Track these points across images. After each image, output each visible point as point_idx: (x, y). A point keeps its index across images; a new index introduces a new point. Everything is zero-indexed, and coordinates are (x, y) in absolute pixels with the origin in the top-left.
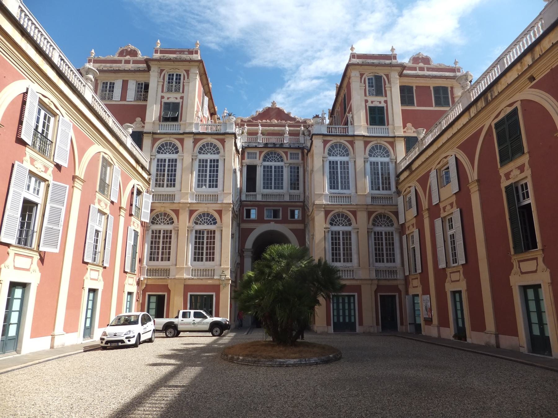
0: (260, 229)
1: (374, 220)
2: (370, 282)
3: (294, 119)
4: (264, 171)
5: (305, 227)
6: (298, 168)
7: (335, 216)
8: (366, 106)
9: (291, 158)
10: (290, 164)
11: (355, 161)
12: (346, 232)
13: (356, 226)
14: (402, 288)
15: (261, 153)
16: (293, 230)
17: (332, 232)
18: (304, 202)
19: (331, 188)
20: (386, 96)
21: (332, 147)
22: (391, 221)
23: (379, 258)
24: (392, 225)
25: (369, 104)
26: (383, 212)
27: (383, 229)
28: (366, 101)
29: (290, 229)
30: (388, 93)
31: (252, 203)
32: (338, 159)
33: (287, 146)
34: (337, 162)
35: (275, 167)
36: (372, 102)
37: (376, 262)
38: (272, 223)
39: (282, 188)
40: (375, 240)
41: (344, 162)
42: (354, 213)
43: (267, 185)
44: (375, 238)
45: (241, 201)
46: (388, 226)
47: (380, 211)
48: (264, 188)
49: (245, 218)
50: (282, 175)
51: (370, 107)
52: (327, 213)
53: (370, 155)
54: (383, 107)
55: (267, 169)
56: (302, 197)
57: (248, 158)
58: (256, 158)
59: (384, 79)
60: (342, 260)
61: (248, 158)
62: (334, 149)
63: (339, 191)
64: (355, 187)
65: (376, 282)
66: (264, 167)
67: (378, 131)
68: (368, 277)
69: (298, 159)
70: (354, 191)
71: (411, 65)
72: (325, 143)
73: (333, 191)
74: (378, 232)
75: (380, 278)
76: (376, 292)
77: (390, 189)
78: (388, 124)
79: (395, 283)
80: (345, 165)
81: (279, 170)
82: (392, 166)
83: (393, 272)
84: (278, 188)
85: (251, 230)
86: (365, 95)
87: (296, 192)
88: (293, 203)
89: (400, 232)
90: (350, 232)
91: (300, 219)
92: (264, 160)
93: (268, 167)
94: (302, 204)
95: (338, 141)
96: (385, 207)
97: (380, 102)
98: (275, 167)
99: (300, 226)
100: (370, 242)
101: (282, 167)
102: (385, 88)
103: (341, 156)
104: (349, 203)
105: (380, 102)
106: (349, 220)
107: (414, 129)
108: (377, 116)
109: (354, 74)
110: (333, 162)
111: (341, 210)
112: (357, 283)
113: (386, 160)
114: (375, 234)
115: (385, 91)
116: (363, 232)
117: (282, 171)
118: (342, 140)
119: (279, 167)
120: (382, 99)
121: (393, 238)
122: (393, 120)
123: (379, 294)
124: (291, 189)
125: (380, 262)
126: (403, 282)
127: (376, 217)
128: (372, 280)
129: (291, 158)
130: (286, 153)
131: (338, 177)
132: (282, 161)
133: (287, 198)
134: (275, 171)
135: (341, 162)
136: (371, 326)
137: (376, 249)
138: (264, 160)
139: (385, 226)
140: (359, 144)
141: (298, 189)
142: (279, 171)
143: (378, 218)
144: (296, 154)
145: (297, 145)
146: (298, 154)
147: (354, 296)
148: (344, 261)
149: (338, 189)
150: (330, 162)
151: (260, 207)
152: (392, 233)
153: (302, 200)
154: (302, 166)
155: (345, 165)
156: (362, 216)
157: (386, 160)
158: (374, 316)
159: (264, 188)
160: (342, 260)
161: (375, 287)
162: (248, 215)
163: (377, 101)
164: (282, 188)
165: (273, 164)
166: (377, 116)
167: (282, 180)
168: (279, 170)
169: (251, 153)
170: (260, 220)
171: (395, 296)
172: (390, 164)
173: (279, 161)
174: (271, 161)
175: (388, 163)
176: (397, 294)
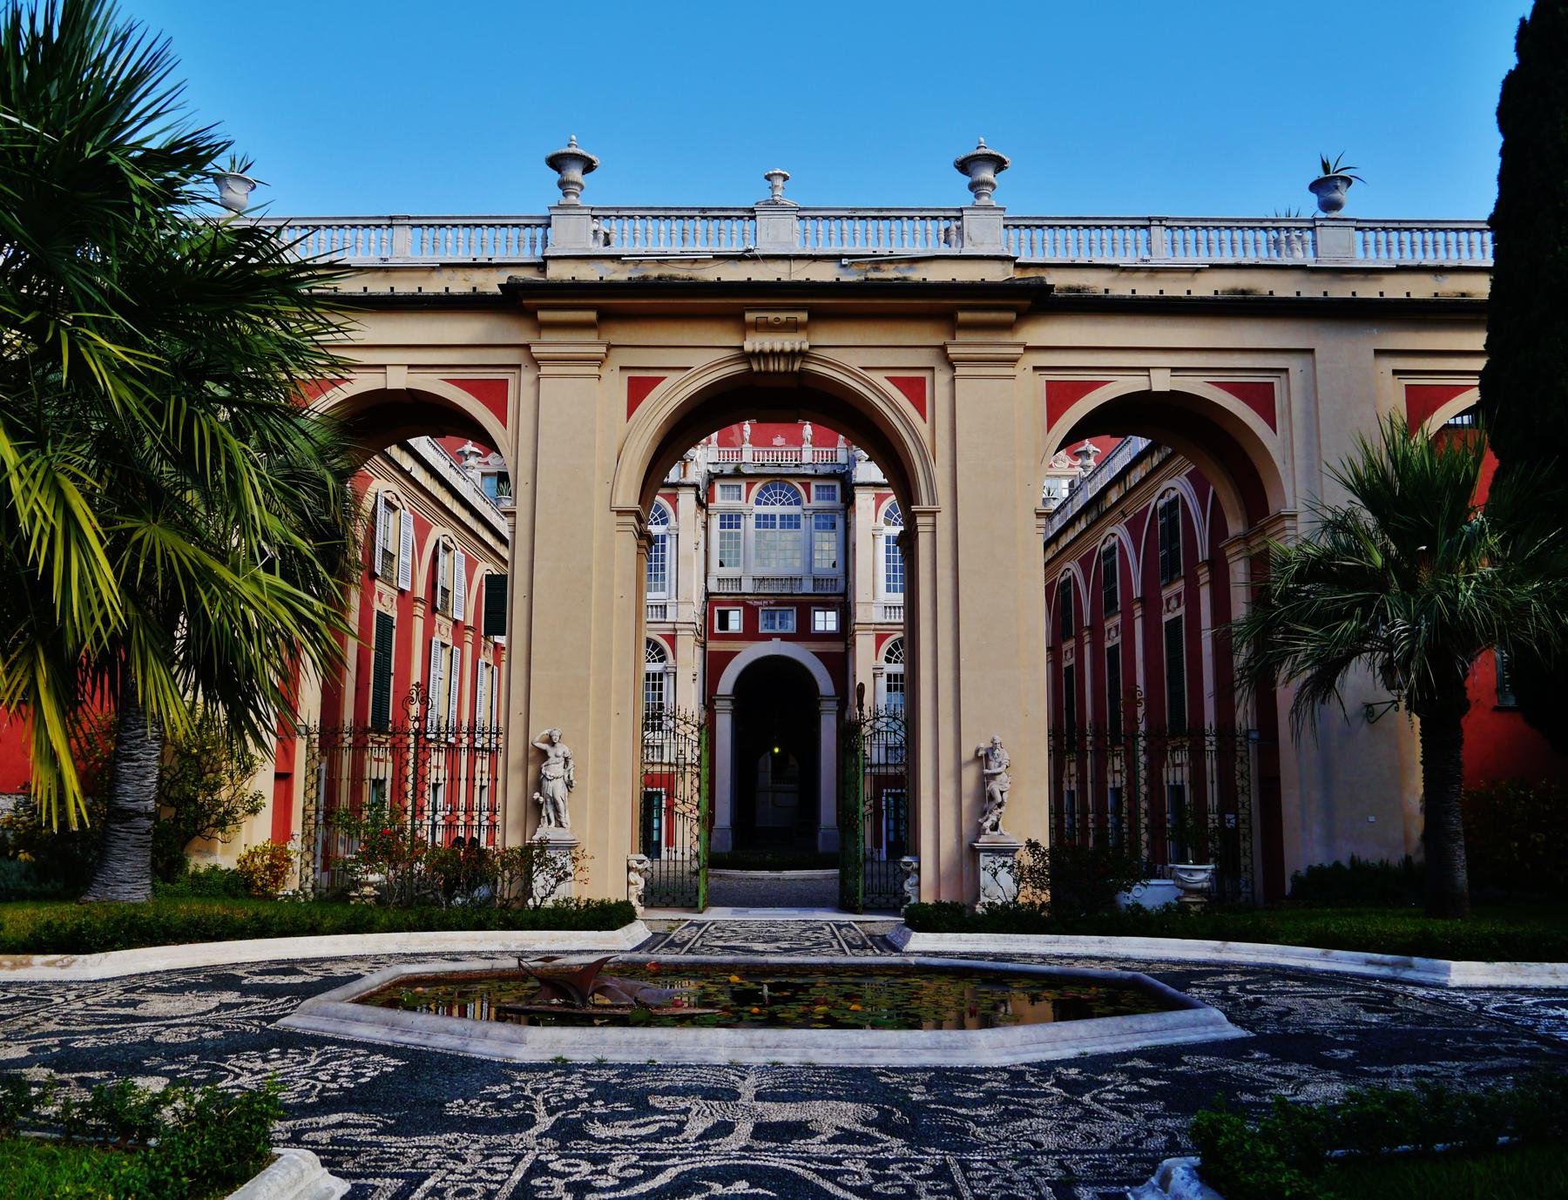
0: (751, 652)
5: (847, 649)
7: (895, 645)
9: (818, 498)
10: (816, 510)
15: (750, 486)
19: (888, 590)
38: (776, 641)
45: (708, 595)
49: (717, 630)
52: (880, 639)
56: (842, 583)
66: (758, 517)
85: (731, 655)
93: (766, 516)
98: (782, 517)
99: (837, 647)
101: (798, 517)
129: (818, 498)
130: (807, 487)
132: (798, 502)
133: (808, 587)
138: (758, 502)
145: (828, 469)
153: (840, 590)
162: (724, 623)
165: (777, 510)
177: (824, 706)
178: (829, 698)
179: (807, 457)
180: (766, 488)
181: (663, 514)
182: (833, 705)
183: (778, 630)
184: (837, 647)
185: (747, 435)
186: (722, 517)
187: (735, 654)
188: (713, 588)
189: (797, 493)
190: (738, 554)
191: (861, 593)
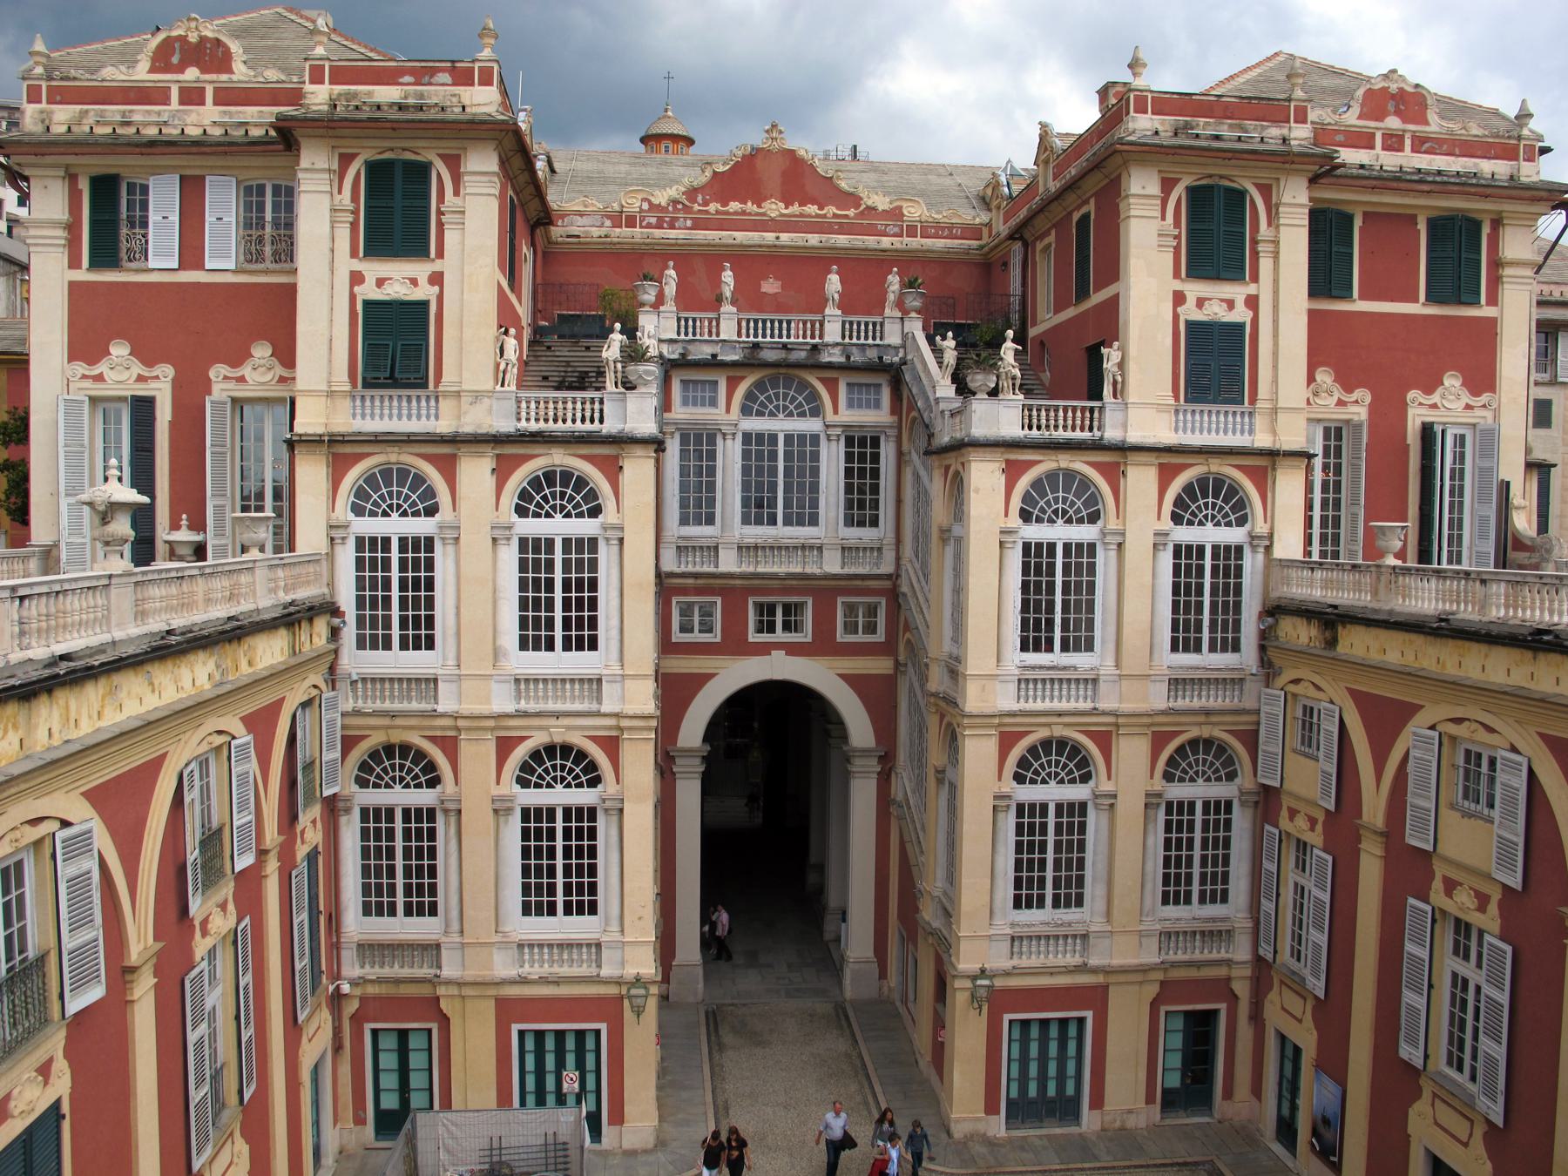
0: (734, 675)
1: (1171, 762)
2: (1139, 977)
3: (852, 199)
4: (746, 455)
6: (875, 442)
7: (1032, 750)
8: (1176, 317)
9: (850, 405)
10: (846, 427)
11: (1120, 545)
12: (1071, 805)
13: (1106, 786)
14: (1242, 989)
15: (732, 384)
16: (851, 680)
17: (1020, 809)
18: (894, 577)
19: (1024, 648)
20: (1255, 278)
21: (1037, 484)
22: (1230, 761)
23: (1174, 894)
24: (1231, 777)
25: (1190, 312)
26: (1206, 735)
27: (1198, 791)
28: (1179, 298)
29: (840, 675)
30: (1265, 264)
31: (700, 581)
32: (1059, 533)
33: (836, 357)
34: (1052, 547)
35: (789, 438)
36: (1200, 303)
37: (1165, 902)
38: (778, 654)
39: (814, 521)
40: (1168, 829)
41: (1079, 546)
42: (1104, 740)
43: (758, 508)
44: (1168, 824)
45: (659, 575)
46: (1219, 779)
47: (1194, 732)
48: (746, 521)
49: (677, 636)
50: (815, 472)
51: (1191, 325)
52: (1007, 741)
53: (1176, 519)
54: (1241, 326)
55: (757, 447)
56: (889, 555)
57: (685, 403)
58: (713, 403)
59: (1253, 202)
60: (1049, 900)
61: (685, 403)
62: (1043, 495)
63: (1057, 657)
64: (1111, 646)
65: (1160, 976)
66: (747, 437)
67: (1213, 429)
68: (1135, 961)
69: (877, 405)
70: (1110, 662)
71: (1351, 118)
72: (1013, 472)
73: (1033, 658)
74: (1180, 804)
75: (1172, 957)
76: (1154, 1005)
77: (1236, 648)
78: (1253, 401)
79: (1222, 972)
80: (1082, 555)
81: (804, 450)
82: (1252, 564)
83: (1216, 935)
84: (801, 523)
85: (702, 679)
86: (1177, 275)
87: (866, 534)
88: (859, 583)
89: (1256, 803)
90: (1083, 806)
91: (880, 636)
92: (746, 411)
94: (887, 584)
95: (1063, 465)
96: (1214, 719)
97: (1231, 304)
98: (789, 438)
99: (879, 666)
100: (1150, 841)
101: (815, 439)
102: (1254, 242)
103: (1069, 521)
104: (1089, 705)
105: (1231, 304)
106: (1084, 763)
107: (1338, 393)
108: (1215, 363)
109: (1142, 185)
110: (1039, 545)
111: (1059, 732)
112: (1100, 979)
113: (1233, 535)
114: (1169, 811)
115: (1255, 255)
116: (1131, 806)
117: (815, 456)
118: (1079, 464)
119: (802, 437)
120: (1238, 292)
121: (1228, 823)
122: (1275, 381)
123: (1163, 1009)
124: (849, 522)
125: (1176, 902)
126: (1248, 972)
127: (1180, 750)
128: (1144, 970)
129: (850, 405)
130: (832, 386)
131: (1055, 604)
132: (816, 412)
133: (832, 564)
134: (788, 456)
135: (1067, 546)
136: (1130, 1112)
137: (1167, 860)
138: (746, 411)
139: (1208, 780)
140: (1141, 479)
141: (874, 523)
142: (802, 455)
143: (1188, 754)
144: (868, 385)
146: (879, 385)
147: (1081, 1021)
148: (1056, 905)
149: (1050, 649)
150: (1026, 547)
151: (732, 590)
152: (1229, 804)
153: (887, 568)
154: (893, 432)
155: (1082, 555)
156: (1132, 753)
157: (1233, 535)
158: (1143, 1076)
159: (746, 521)
160: (1049, 900)
161: (1152, 990)
163: (1218, 302)
164: (814, 521)
165: (781, 425)
166: (1215, 363)
167: (815, 488)
168: (804, 450)
169: (695, 382)
170: (735, 645)
171: (1215, 1012)
172: (1247, 552)
173: (802, 415)
174: (772, 414)
175: (1239, 549)
176: (1223, 1007)
177: (858, 764)
178: (865, 752)
179: (833, 332)
180: (760, 386)
181: (592, 495)
182: (874, 765)
183: (780, 635)
184: (879, 666)
185: (727, 291)
186: (684, 440)
187: (710, 676)
188: (670, 564)
189: (814, 396)
190: (711, 502)
191: (977, 660)
